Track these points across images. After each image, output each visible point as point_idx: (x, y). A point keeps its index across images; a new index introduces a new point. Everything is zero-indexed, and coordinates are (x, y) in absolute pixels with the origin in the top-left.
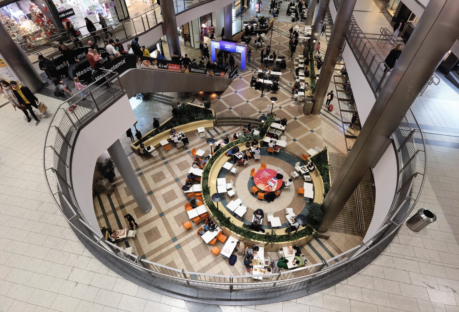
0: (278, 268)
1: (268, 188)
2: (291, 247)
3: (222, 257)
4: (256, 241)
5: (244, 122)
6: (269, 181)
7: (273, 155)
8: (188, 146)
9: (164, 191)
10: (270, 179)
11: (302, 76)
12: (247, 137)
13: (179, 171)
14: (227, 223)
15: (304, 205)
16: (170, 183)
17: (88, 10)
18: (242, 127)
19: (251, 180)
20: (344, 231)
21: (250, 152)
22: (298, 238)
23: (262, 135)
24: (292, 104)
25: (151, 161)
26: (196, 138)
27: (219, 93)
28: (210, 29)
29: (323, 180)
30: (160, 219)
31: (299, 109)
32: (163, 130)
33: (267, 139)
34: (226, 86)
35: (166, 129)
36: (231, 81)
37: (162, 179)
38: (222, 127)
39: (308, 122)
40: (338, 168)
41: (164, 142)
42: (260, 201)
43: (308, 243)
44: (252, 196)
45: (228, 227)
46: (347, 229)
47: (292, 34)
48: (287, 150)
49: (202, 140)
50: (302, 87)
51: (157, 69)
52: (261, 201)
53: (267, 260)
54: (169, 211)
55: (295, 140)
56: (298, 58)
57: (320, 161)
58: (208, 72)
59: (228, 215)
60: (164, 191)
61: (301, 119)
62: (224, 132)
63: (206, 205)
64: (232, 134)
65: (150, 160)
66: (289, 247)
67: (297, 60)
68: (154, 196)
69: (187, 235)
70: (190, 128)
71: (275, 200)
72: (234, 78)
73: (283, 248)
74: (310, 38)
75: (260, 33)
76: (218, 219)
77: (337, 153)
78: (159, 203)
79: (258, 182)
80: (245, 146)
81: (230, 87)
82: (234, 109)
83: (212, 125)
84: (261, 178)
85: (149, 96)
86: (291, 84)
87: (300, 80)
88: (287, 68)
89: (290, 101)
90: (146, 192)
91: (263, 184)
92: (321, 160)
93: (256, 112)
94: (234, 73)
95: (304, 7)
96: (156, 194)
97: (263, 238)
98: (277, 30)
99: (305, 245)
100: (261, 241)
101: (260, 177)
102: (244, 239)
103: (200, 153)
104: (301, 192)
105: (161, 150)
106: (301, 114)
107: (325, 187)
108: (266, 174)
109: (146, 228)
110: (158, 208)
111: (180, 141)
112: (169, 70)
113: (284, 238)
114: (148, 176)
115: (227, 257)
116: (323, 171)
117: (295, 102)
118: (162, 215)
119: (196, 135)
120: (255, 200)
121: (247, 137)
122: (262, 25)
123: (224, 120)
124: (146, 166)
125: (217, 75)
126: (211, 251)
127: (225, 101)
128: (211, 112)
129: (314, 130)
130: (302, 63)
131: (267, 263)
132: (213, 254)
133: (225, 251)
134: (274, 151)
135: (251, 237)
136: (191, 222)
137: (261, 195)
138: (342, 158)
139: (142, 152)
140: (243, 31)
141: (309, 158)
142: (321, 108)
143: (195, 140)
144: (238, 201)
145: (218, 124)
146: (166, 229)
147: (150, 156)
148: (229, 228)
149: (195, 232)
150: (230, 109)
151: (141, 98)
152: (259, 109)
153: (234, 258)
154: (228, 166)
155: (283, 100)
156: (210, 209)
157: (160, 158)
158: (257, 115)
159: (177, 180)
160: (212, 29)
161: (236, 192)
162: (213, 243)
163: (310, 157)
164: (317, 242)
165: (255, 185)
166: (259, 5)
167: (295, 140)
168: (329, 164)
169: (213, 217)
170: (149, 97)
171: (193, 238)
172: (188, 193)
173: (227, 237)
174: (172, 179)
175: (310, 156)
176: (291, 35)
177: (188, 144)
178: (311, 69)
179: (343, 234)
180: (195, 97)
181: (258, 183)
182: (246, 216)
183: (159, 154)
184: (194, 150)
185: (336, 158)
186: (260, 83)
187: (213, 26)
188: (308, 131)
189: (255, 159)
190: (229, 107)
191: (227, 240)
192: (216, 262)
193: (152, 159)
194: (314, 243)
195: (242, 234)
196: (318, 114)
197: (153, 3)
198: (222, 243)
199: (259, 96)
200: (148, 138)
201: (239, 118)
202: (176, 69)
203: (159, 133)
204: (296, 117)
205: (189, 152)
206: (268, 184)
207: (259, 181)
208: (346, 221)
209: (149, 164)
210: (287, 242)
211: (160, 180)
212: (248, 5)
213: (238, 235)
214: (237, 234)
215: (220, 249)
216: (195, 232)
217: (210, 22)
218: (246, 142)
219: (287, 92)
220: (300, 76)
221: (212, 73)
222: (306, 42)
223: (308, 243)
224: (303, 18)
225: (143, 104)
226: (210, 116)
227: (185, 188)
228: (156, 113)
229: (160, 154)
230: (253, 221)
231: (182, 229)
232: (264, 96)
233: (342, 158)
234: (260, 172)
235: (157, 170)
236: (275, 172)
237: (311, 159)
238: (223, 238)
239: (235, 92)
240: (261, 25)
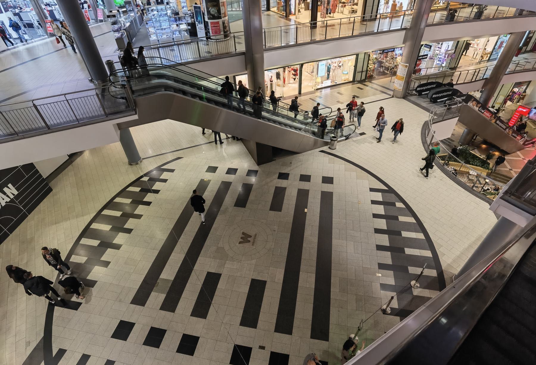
17: (431, 56)
34: (514, 150)
36: (523, 149)
58: (507, 130)
72: (528, 147)
81: (518, 153)
83: (484, 174)
94: (530, 142)
112: (483, 115)
123: (499, 176)
125: (513, 136)
128: (489, 164)
160: (522, 95)
180: (476, 148)
187: (526, 92)
197: (481, 60)
221: (511, 132)
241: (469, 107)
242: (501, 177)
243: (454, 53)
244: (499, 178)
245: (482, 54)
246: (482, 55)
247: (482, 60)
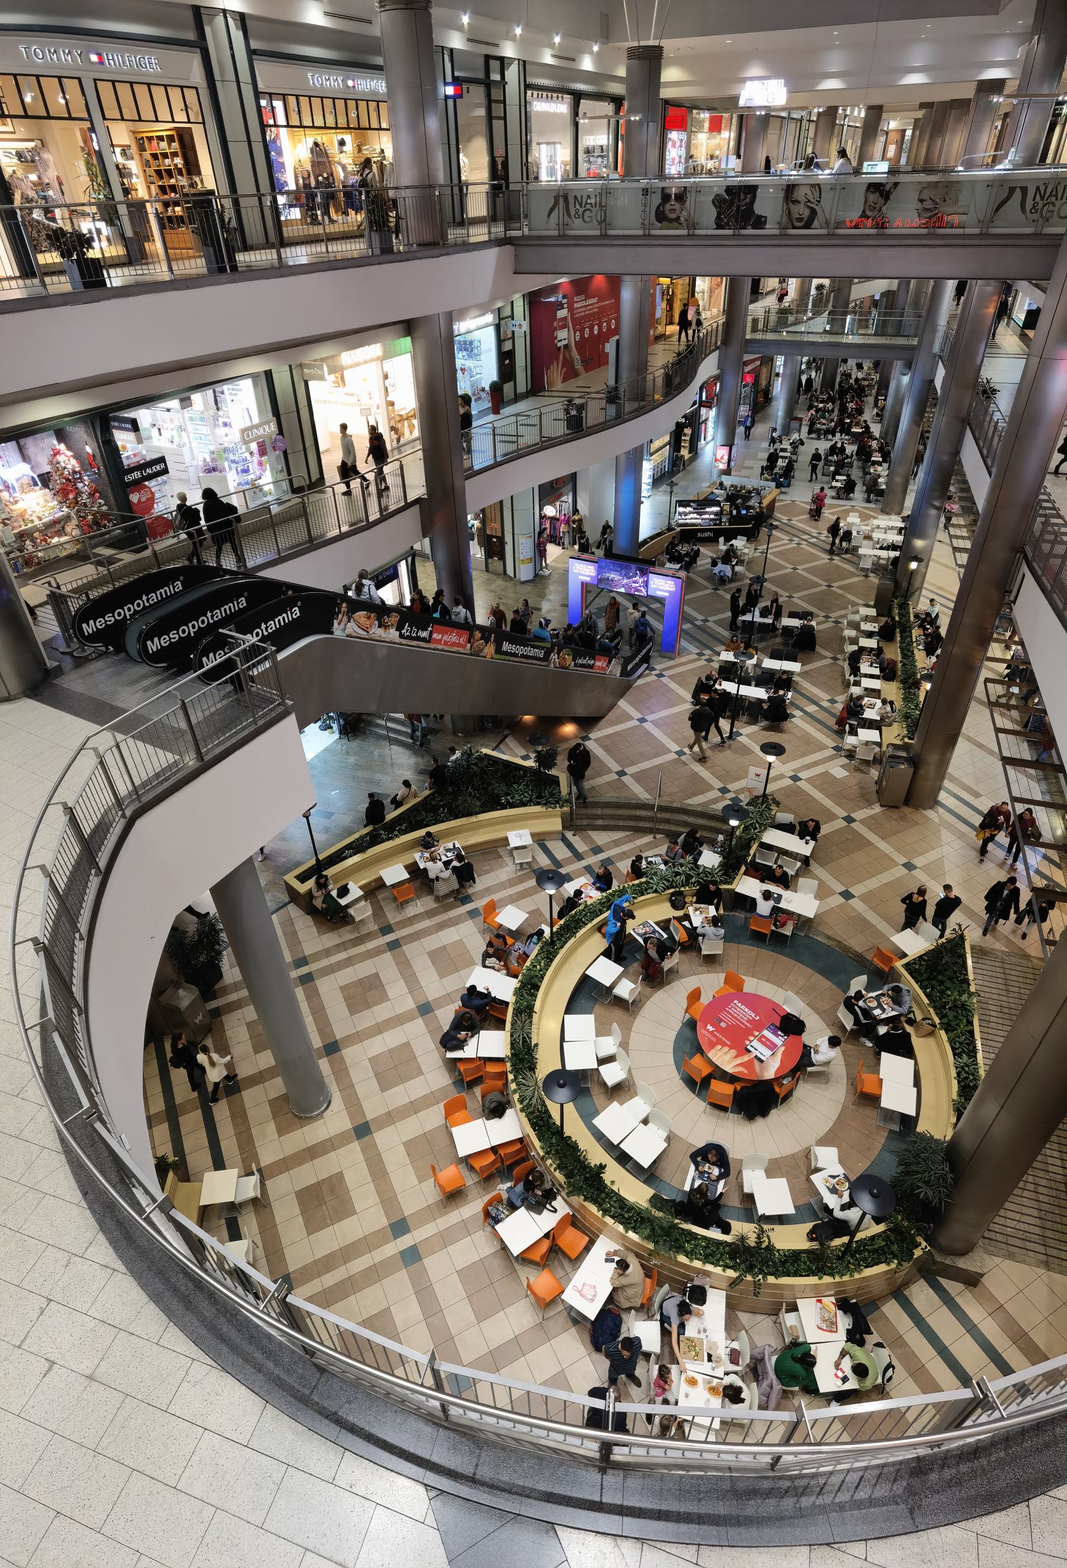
0: (778, 1386)
1: (748, 1065)
2: (829, 1301)
3: (565, 1313)
4: (697, 1264)
5: (667, 821)
6: (752, 1038)
7: (769, 945)
8: (470, 891)
9: (378, 1045)
10: (757, 1033)
11: (872, 676)
12: (677, 874)
13: (436, 977)
14: (591, 1186)
15: (880, 1140)
16: (400, 1020)
17: (208, 460)
18: (658, 836)
19: (688, 1032)
20: (1044, 1258)
21: (684, 926)
22: (858, 1268)
23: (731, 866)
24: (838, 770)
25: (346, 934)
26: (501, 867)
27: (587, 723)
28: (567, 522)
29: (953, 1049)
30: (355, 1146)
31: (861, 788)
32: (396, 833)
33: (748, 886)
34: (609, 700)
35: (405, 832)
36: (629, 686)
37: (376, 1003)
38: (590, 833)
39: (896, 833)
40: (1006, 1005)
41: (394, 873)
42: (717, 1112)
43: (898, 1293)
44: (687, 1092)
45: (594, 1201)
46: (1054, 1252)
47: (837, 541)
48: (820, 928)
49: (519, 874)
50: (870, 714)
51: (398, 639)
52: (722, 1114)
53: (735, 1345)
54: (390, 1118)
55: (847, 895)
56: (857, 618)
57: (940, 977)
58: (554, 657)
59: (596, 1155)
60: (378, 1045)
61: (871, 823)
62: (597, 850)
63: (522, 1110)
64: (623, 859)
65: (341, 931)
66: (824, 1299)
67: (855, 626)
68: (342, 1060)
69: (446, 1217)
70: (481, 830)
71: (774, 1113)
72: (639, 677)
73: (799, 1302)
74: (897, 554)
75: (730, 535)
76: (559, 1167)
77: (1002, 952)
78: (358, 1089)
79: (714, 1040)
80: (668, 905)
81: (622, 703)
82: (636, 777)
83: (555, 824)
84: (723, 1025)
85: (362, 721)
86: (832, 701)
87: (866, 689)
88: (818, 649)
89: (831, 758)
90: (317, 1042)
91: (731, 1047)
92: (943, 975)
93: (710, 788)
95: (877, 457)
96: (349, 1053)
97: (722, 1255)
98: (787, 529)
99: (884, 1298)
100: (716, 1265)
101: (721, 1021)
102: (651, 1253)
103: (511, 918)
104: (869, 1088)
105: (383, 899)
106: (869, 804)
107: (959, 1074)
108: (742, 1012)
109: (307, 1175)
110: (353, 1104)
111: (447, 874)
112: (432, 646)
113: (805, 1263)
114: (329, 988)
115: (585, 1318)
116: (951, 1015)
117: (845, 761)
118: (362, 1131)
119: (500, 857)
120: (697, 1105)
121: (677, 874)
122: (739, 512)
123: (599, 812)
124: (328, 952)
125: (582, 666)
126: (529, 1286)
127: (605, 748)
128: (555, 781)
129: (918, 861)
130: (870, 635)
131: (734, 1356)
132: (533, 1301)
133: (580, 1292)
134: (773, 928)
135: (680, 1249)
136: (463, 1168)
137: (722, 1089)
138: (1020, 969)
139: (318, 903)
140: (674, 529)
141: (899, 965)
142: (940, 789)
143: (498, 872)
144: (638, 1106)
145: (578, 822)
146: (371, 1187)
147: (344, 917)
148: (600, 1207)
149: (473, 1207)
150: (621, 773)
151: (335, 726)
153: (610, 1323)
154: (606, 971)
155: (804, 754)
156: (534, 1126)
157: (376, 927)
158: (715, 801)
159: (425, 1009)
160: (574, 522)
161: (629, 1070)
162: (536, 1256)
163: (905, 961)
164: (931, 1291)
165: (699, 1050)
166: (730, 450)
167: (847, 895)
168: (972, 989)
169: (542, 1158)
170: (362, 725)
171: (464, 1229)
172: (460, 1060)
173: (587, 1239)
174: (409, 1004)
175: (905, 955)
176: (833, 543)
177: (470, 886)
178: (904, 656)
179: (1041, 1271)
180: (506, 732)
181: (712, 1045)
182: (663, 1164)
183: (374, 914)
184: (492, 908)
185: (998, 970)
186: (726, 694)
188: (894, 863)
189: (704, 952)
190: (616, 767)
191: (587, 1249)
192: (542, 1332)
193: (349, 927)
194: (921, 1294)
195: (647, 1232)
196: (931, 807)
197: (398, 440)
198: (570, 1259)
200: (346, 858)
201: (649, 807)
202: (454, 644)
203: (383, 841)
204: (853, 815)
205: (472, 914)
206: (749, 1051)
207: (715, 1036)
208: (1049, 1216)
209: (337, 945)
210: (813, 1280)
211: (368, 1006)
212: (694, 448)
213: (631, 1235)
214: (626, 1231)
215: (559, 1283)
216: (473, 1207)
217: (570, 500)
218: (672, 890)
219: (819, 726)
220: (866, 676)
221: (569, 659)
222: (884, 568)
223: (898, 1293)
224: (873, 490)
225: (339, 746)
226: (552, 795)
227: (450, 1041)
228: (378, 776)
229: (378, 912)
230: (687, 1188)
231: (429, 1193)
232: (740, 738)
233: (1020, 969)
234: (720, 1003)
235: (363, 970)
236: (775, 1008)
237: (907, 966)
238: (573, 1239)
239: (638, 720)
240: (734, 512)
241: (347, 644)
243: (281, 432)
245: (389, 420)
246: (393, 424)
247: (402, 441)
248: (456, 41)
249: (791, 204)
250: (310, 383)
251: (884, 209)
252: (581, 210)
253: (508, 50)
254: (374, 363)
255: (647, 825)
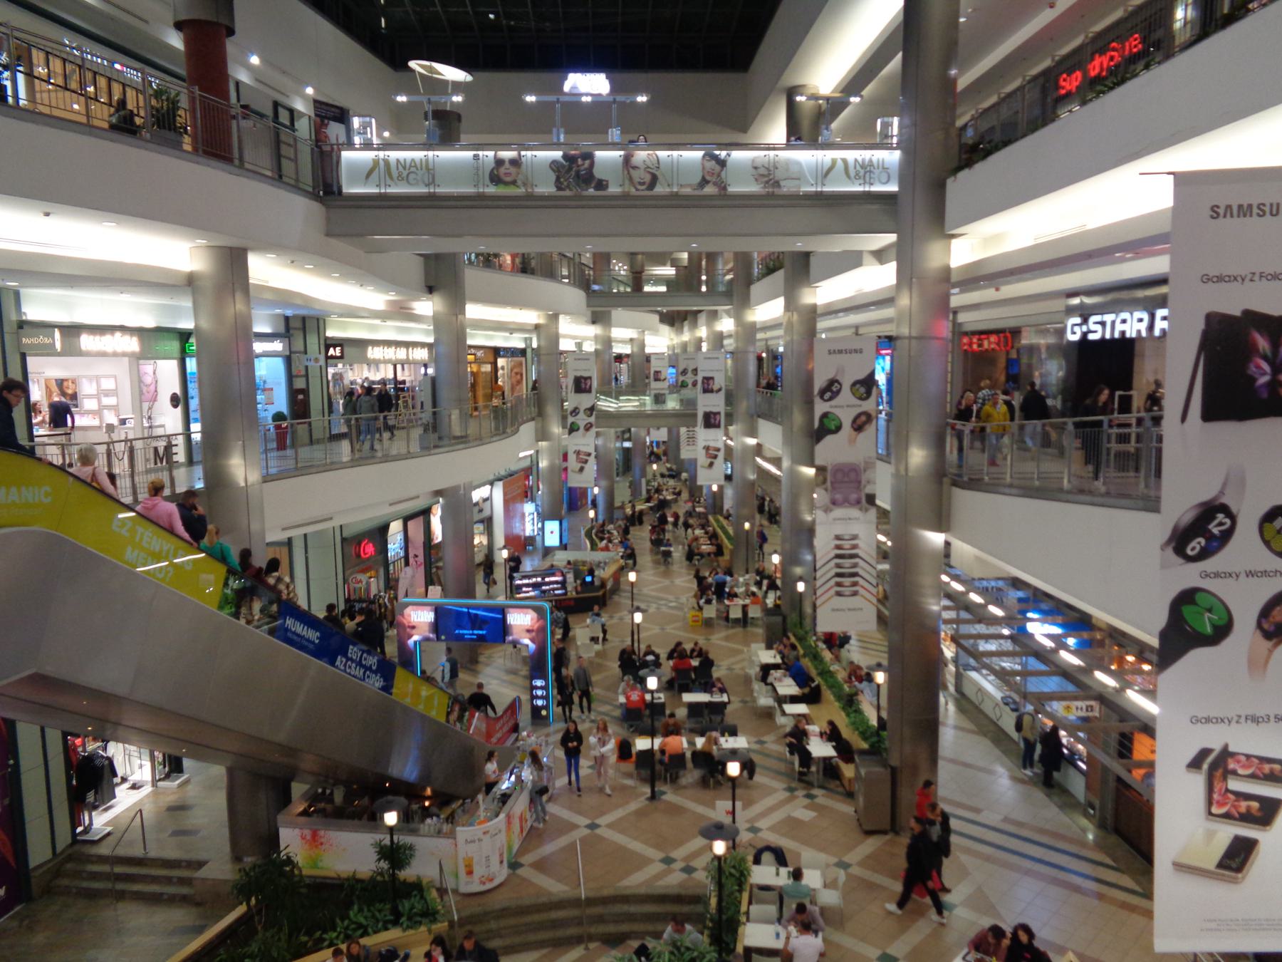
5: (600, 919)
18: (592, 946)
93: (646, 861)
152: (657, 846)
158: (659, 876)
199: (643, 799)
232: (664, 797)
242: (504, 923)
244: (501, 937)
248: (244, 77)
249: (631, 170)
250: (29, 359)
251: (723, 174)
252: (405, 173)
253: (299, 106)
254: (126, 360)
255: (572, 931)
